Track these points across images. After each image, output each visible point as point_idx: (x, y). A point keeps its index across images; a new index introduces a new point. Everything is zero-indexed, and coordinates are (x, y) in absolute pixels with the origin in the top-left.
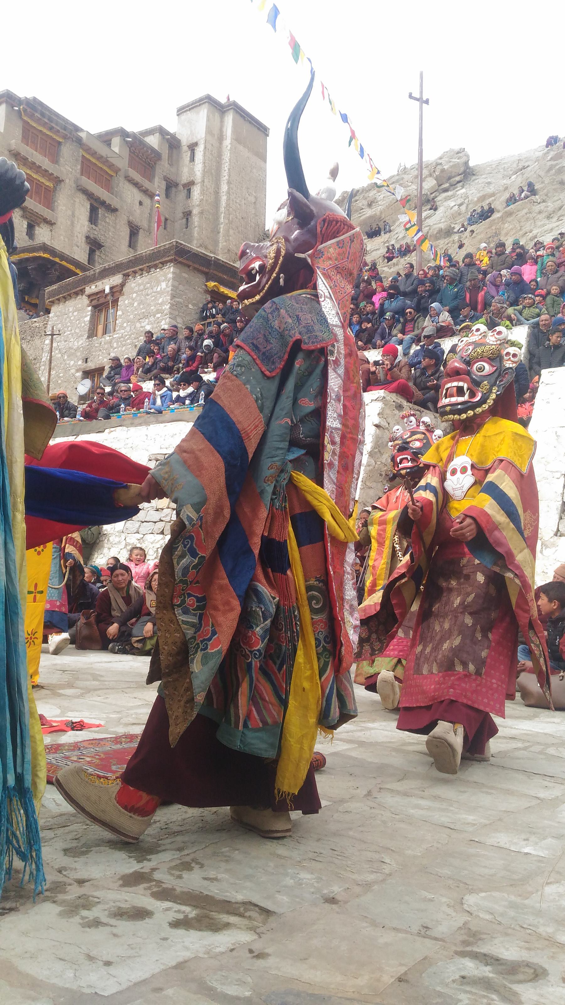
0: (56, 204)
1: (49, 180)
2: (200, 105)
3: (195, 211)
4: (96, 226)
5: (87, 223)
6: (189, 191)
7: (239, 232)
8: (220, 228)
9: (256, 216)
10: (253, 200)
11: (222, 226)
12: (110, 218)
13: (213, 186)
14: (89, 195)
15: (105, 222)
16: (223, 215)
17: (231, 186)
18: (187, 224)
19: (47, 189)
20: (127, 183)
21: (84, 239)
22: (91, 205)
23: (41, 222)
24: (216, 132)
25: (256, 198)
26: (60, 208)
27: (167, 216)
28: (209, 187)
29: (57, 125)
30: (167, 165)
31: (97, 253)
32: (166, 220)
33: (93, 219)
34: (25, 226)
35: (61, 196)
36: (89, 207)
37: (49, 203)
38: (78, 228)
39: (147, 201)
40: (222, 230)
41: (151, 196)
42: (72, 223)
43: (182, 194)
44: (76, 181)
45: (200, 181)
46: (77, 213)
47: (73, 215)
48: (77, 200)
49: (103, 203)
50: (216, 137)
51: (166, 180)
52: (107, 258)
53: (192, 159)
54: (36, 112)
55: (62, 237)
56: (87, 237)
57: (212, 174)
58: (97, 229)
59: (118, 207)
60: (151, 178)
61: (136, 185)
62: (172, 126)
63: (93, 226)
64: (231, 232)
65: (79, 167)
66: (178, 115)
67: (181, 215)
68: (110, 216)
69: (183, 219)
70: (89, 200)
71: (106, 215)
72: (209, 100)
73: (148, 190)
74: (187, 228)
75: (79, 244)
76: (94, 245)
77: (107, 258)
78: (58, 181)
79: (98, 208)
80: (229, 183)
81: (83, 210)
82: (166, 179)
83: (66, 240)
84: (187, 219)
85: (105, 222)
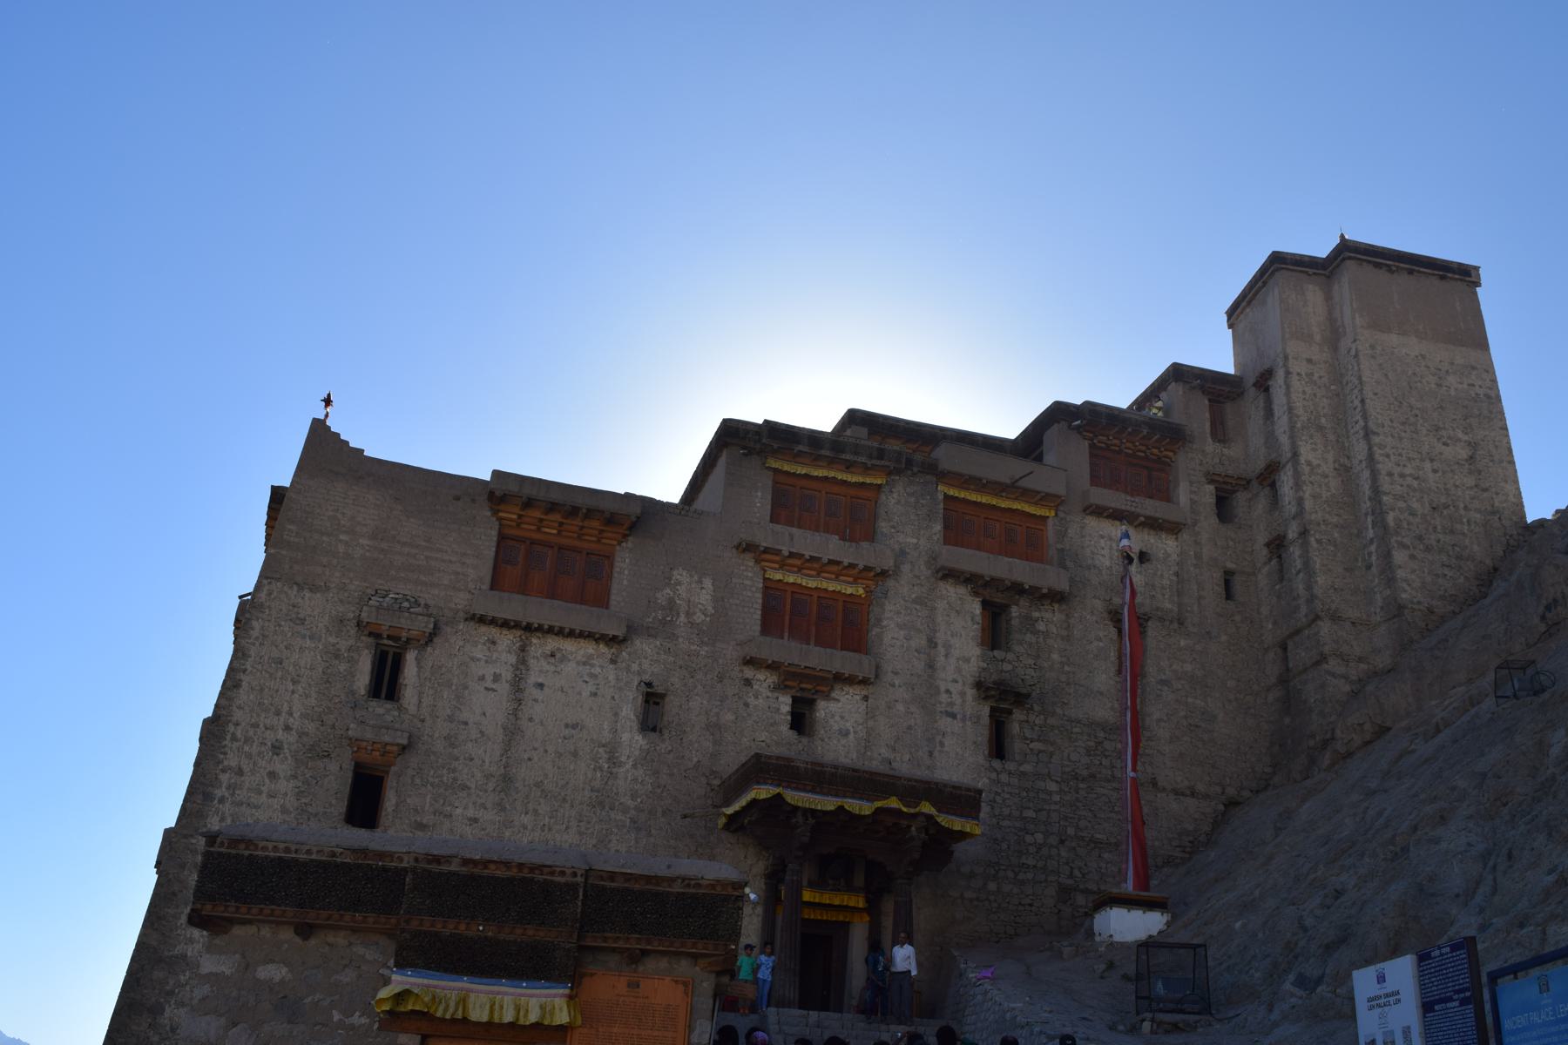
0: (876, 630)
1: (856, 581)
2: (1265, 283)
3: (1291, 535)
4: (1009, 650)
5: (974, 651)
6: (1273, 485)
7: (1428, 549)
8: (1370, 554)
9: (1485, 490)
10: (1464, 453)
11: (1373, 548)
12: (1049, 618)
13: (1330, 457)
15: (1036, 632)
16: (1369, 519)
17: (1376, 440)
18: (1281, 571)
20: (1092, 523)
21: (971, 693)
22: (985, 604)
23: (832, 688)
25: (1473, 446)
26: (887, 639)
27: (1230, 565)
28: (1315, 462)
29: (856, 453)
30: (1211, 447)
31: (1018, 715)
34: (786, 708)
35: (889, 607)
36: (976, 608)
39: (1165, 546)
40: (1374, 558)
41: (1174, 529)
42: (931, 666)
45: (1289, 455)
46: (940, 637)
47: (932, 643)
48: (941, 605)
49: (1018, 589)
50: (1318, 338)
51: (1211, 482)
52: (1051, 721)
53: (1269, 413)
54: (798, 443)
55: (901, 707)
56: (979, 685)
57: (1320, 428)
58: (1010, 656)
59: (1063, 585)
60: (1164, 494)
61: (1117, 516)
62: (1219, 356)
63: (996, 653)
64: (1399, 557)
65: (938, 527)
66: (1230, 326)
67: (1265, 551)
68: (1048, 615)
69: (1270, 560)
70: (976, 594)
71: (1036, 614)
72: (1278, 263)
73: (1156, 519)
74: (1281, 580)
75: (956, 709)
76: (1003, 699)
77: (1051, 721)
79: (1004, 608)
80: (1368, 434)
82: (1211, 478)
83: (913, 709)
84: (1280, 557)
85: (1036, 632)
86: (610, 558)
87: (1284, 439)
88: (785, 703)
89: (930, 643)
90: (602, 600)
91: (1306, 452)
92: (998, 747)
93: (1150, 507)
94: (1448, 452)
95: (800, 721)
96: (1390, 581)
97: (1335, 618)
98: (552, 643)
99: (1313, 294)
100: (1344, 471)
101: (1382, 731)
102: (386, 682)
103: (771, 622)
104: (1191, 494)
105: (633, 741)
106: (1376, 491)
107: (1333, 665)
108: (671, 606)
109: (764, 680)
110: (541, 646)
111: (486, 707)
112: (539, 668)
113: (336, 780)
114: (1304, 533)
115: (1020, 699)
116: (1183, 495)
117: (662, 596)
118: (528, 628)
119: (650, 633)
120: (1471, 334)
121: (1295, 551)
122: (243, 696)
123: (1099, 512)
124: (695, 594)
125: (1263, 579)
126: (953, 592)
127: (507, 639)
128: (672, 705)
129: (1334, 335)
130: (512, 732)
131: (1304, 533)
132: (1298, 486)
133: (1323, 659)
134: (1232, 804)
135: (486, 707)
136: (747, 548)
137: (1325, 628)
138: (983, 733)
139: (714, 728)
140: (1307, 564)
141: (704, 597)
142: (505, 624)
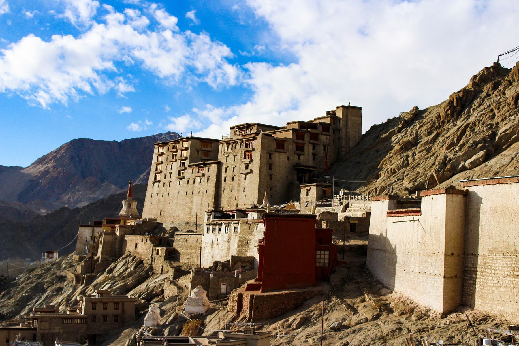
12: (318, 146)
14: (312, 144)
39: (328, 137)
43: (338, 133)
56: (312, 154)
76: (314, 155)
81: (311, 147)
89: (308, 149)
90: (283, 148)
92: (314, 159)
95: (299, 158)
100: (346, 131)
102: (270, 158)
104: (331, 131)
105: (287, 161)
111: (277, 159)
113: (268, 165)
116: (330, 131)
120: (360, 116)
124: (290, 147)
126: (310, 144)
135: (277, 159)
136: (294, 142)
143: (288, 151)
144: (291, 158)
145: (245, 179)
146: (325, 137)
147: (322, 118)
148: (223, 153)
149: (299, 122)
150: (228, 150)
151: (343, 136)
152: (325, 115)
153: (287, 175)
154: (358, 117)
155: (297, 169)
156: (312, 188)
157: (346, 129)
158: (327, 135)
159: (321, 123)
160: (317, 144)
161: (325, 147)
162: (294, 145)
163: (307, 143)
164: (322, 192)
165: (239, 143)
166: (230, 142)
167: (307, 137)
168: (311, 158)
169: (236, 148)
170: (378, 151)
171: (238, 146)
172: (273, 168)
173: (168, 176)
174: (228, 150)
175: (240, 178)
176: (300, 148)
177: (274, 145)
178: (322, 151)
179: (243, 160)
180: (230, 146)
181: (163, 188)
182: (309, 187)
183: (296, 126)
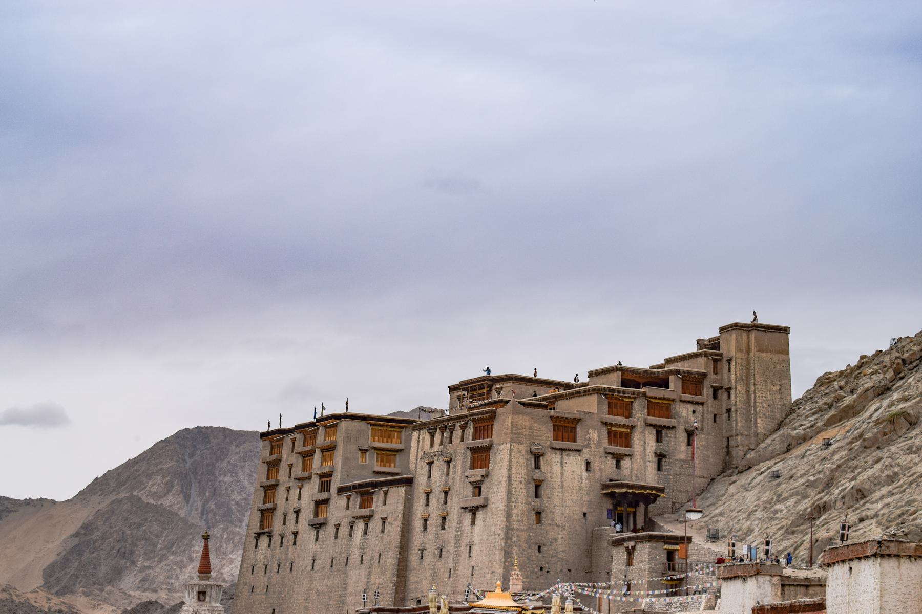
3: (733, 409)
10: (778, 388)
12: (671, 433)
14: (654, 426)
19: (627, 434)
24: (744, 347)
25: (781, 385)
30: (713, 376)
32: (715, 415)
33: (659, 439)
36: (654, 432)
37: (628, 445)
38: (648, 450)
39: (699, 409)
41: (702, 404)
42: (645, 449)
43: (725, 395)
44: (645, 420)
49: (665, 427)
59: (675, 425)
61: (689, 402)
64: (759, 420)
78: (632, 427)
80: (755, 385)
82: (712, 387)
86: (575, 428)
87: (733, 382)
88: (614, 461)
89: (644, 444)
90: (575, 440)
91: (738, 387)
92: (659, 469)
93: (697, 398)
94: (774, 388)
95: (618, 466)
96: (756, 427)
97: (742, 435)
98: (567, 452)
99: (744, 335)
100: (748, 392)
101: (750, 468)
102: (537, 466)
103: (610, 443)
104: (707, 392)
105: (585, 474)
106: (755, 402)
107: (740, 447)
108: (589, 440)
109: (610, 457)
110: (565, 453)
111: (557, 469)
112: (566, 459)
113: (532, 486)
114: (736, 411)
115: (665, 456)
116: (705, 392)
117: (587, 437)
118: (562, 450)
119: (586, 446)
121: (733, 415)
122: (513, 471)
123: (684, 402)
125: (725, 416)
127: (558, 453)
128: (592, 464)
129: (748, 351)
130: (562, 474)
131: (736, 411)
132: (736, 397)
133: (738, 446)
134: (712, 480)
135: (557, 469)
137: (739, 438)
138: (655, 465)
139: (601, 470)
140: (736, 420)
141: (596, 436)
142: (557, 449)
143: (588, 446)
144: (596, 465)
145: (473, 523)
146: (691, 408)
147: (683, 358)
148: (421, 454)
149: (619, 369)
150: (432, 445)
151: (739, 405)
152: (694, 349)
153: (584, 510)
154: (779, 352)
155: (612, 495)
156: (639, 546)
157: (748, 386)
158: (697, 403)
159: (677, 372)
160: (669, 428)
161: (690, 434)
162: (605, 432)
163: (640, 425)
164: (663, 558)
165: (458, 427)
166: (439, 425)
167: (639, 412)
168: (652, 467)
169: (450, 442)
170: (828, 444)
171: (458, 433)
172: (543, 491)
173: (292, 517)
174: (432, 445)
175: (460, 522)
176: (620, 437)
177: (546, 434)
178: (683, 447)
179: (468, 472)
180: (438, 436)
181: (278, 550)
182: (632, 543)
183: (613, 382)
